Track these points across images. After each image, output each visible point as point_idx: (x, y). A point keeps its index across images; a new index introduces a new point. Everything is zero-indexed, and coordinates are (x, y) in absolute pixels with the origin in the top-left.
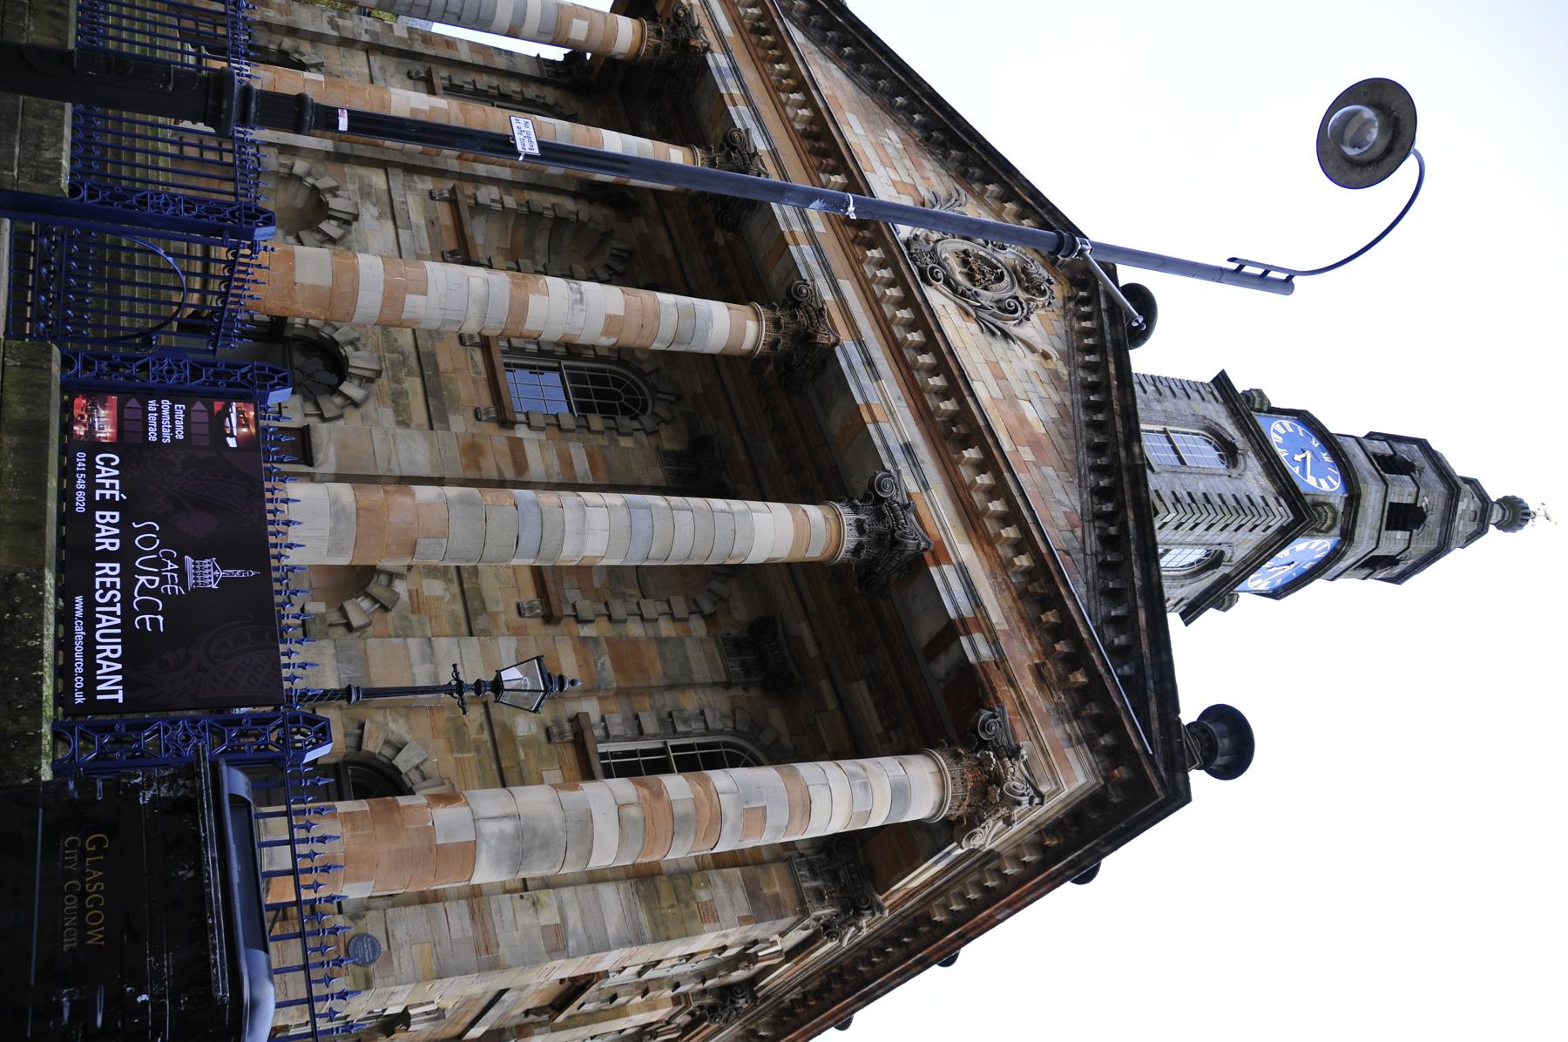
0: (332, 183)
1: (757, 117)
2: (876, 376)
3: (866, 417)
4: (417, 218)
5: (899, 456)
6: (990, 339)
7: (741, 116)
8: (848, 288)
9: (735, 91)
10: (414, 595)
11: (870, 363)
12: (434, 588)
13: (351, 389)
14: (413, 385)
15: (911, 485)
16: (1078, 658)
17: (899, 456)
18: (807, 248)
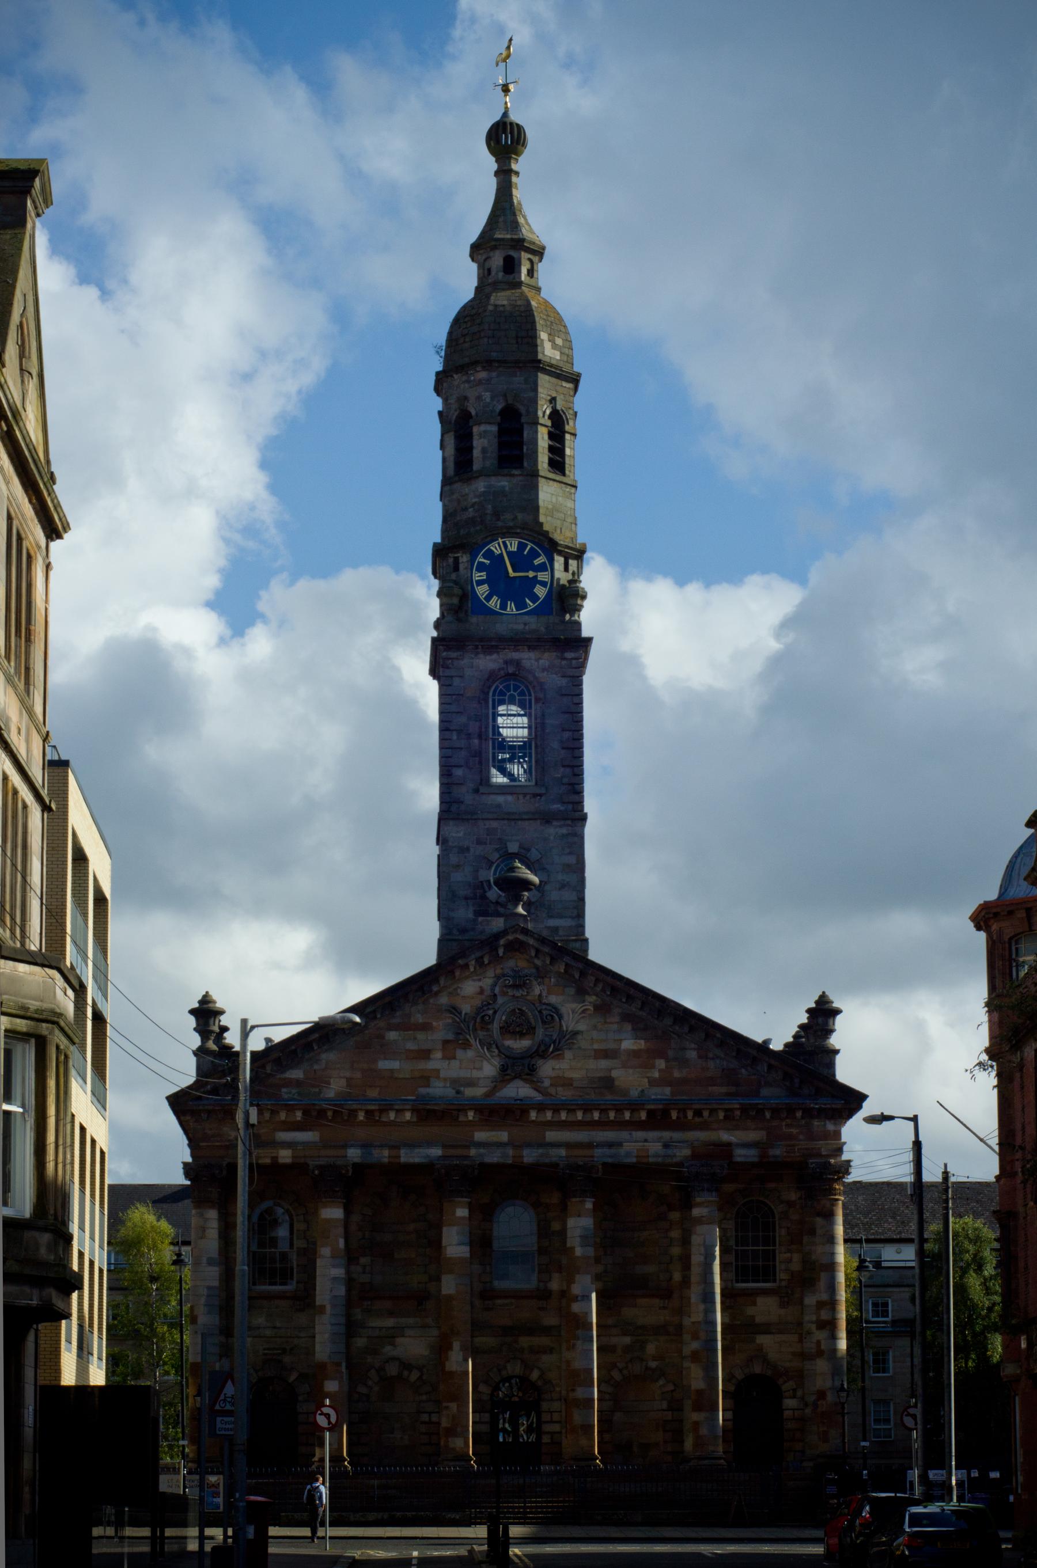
0: (373, 1371)
1: (412, 1145)
2: (620, 1145)
3: (645, 1160)
4: (390, 1322)
5: (670, 1152)
6: (576, 1046)
7: (407, 1156)
8: (551, 1136)
9: (386, 1153)
10: (654, 1359)
11: (610, 1145)
12: (651, 1348)
13: (535, 1375)
14: (525, 1341)
15: (687, 1152)
16: (791, 1111)
17: (670, 1152)
18: (526, 1152)
